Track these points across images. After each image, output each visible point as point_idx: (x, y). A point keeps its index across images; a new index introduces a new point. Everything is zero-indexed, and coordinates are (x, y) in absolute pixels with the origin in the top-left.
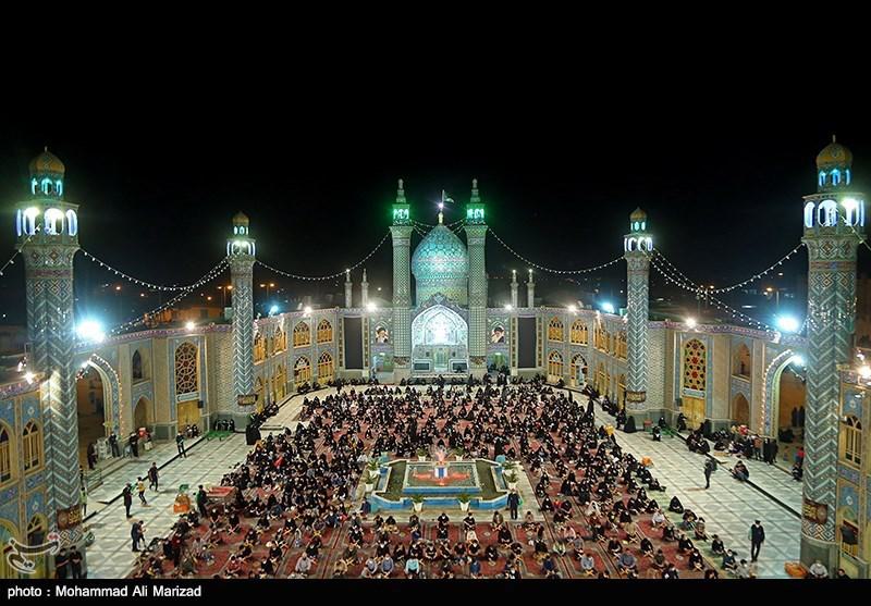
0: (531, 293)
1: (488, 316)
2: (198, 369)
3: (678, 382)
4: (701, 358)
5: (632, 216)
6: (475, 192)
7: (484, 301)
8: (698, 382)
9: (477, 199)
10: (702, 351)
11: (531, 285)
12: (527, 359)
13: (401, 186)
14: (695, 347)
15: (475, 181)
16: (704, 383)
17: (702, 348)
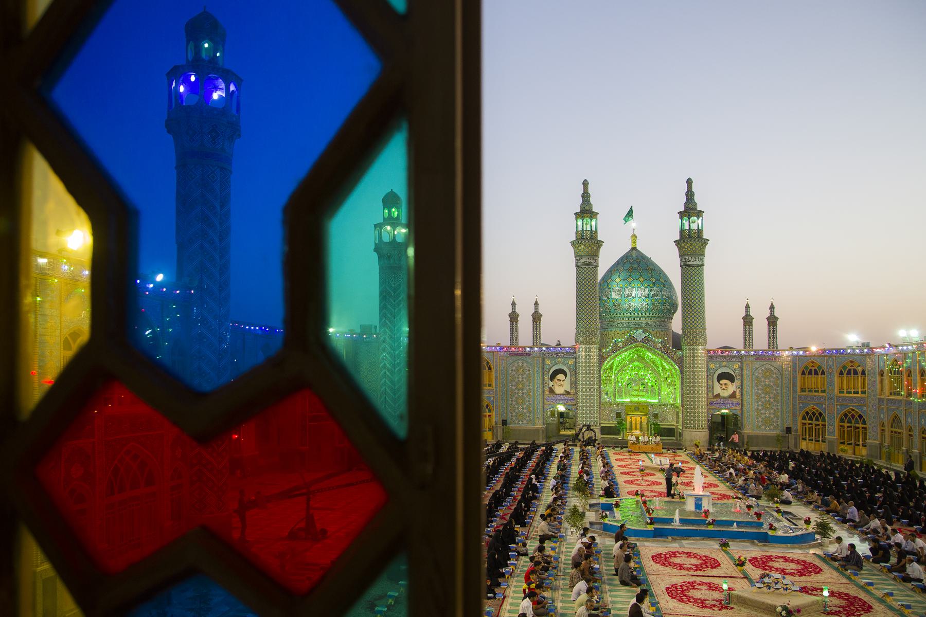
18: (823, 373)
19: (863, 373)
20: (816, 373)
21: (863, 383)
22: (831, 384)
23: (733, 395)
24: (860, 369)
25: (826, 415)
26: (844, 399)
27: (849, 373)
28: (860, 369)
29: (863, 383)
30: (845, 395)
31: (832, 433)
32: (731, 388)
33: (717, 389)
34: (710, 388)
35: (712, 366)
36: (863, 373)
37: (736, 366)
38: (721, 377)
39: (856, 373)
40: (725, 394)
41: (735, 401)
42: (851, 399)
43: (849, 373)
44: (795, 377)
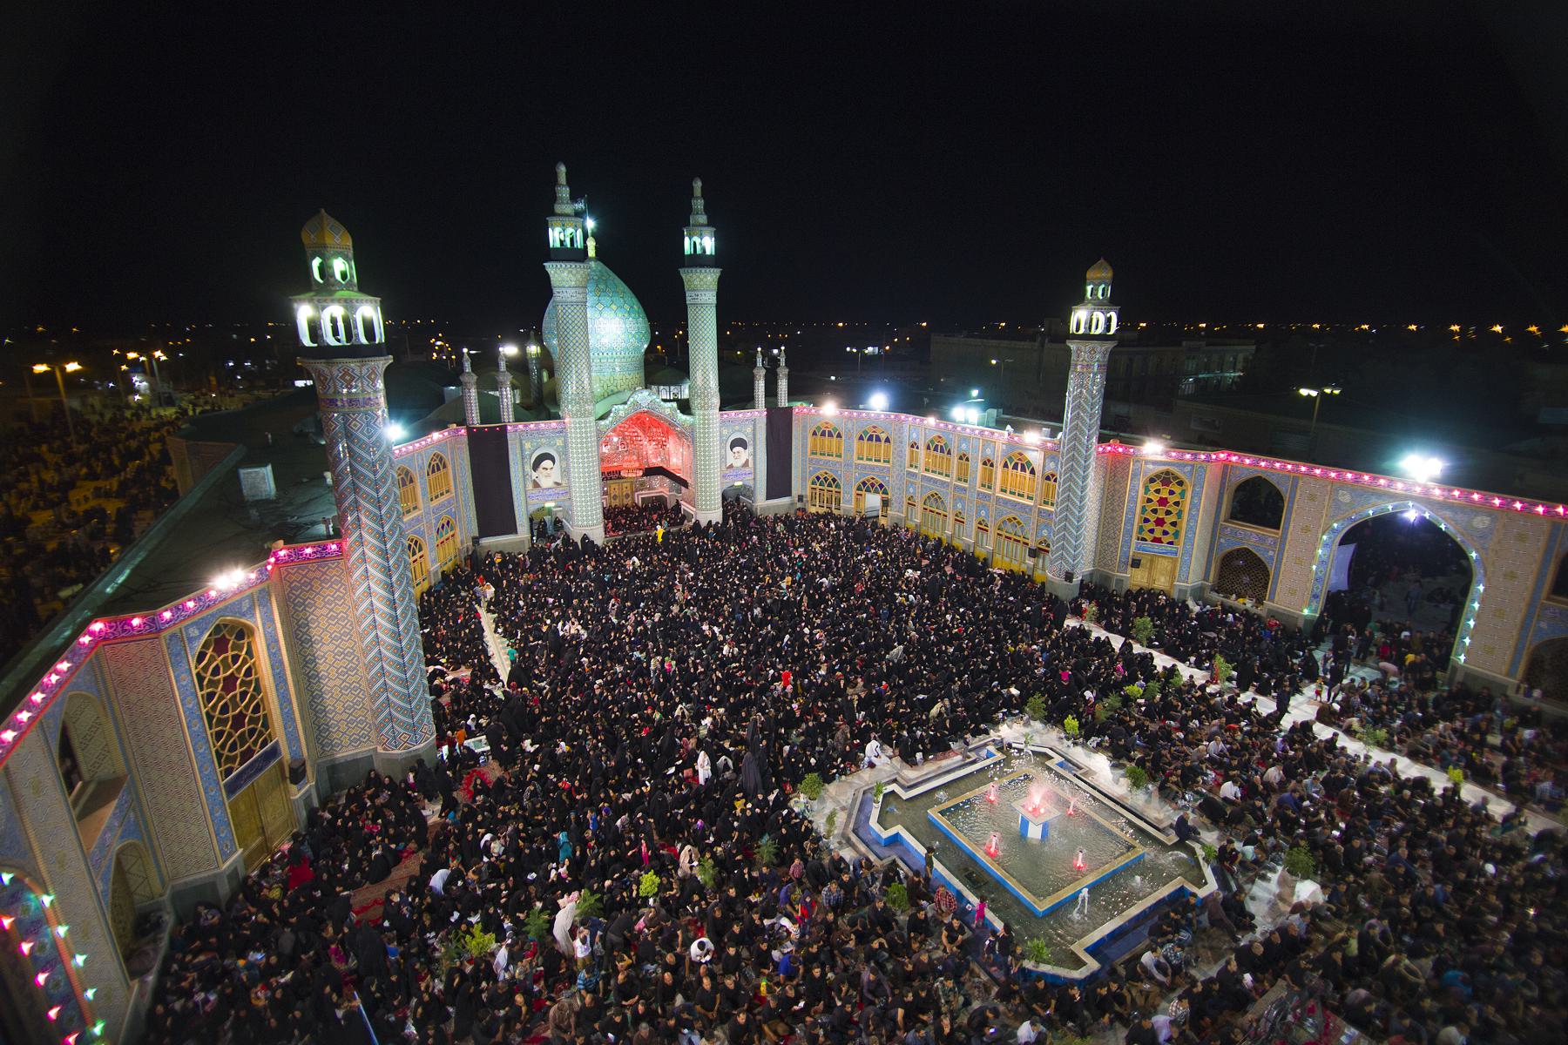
0: (783, 385)
1: (723, 422)
2: (268, 682)
3: (1129, 533)
4: (1172, 499)
5: (1090, 275)
6: (699, 204)
7: (716, 401)
8: (1166, 533)
9: (703, 219)
10: (1177, 489)
11: (783, 372)
12: (779, 483)
13: (562, 178)
14: (1166, 482)
15: (698, 185)
16: (1177, 534)
17: (1181, 483)
18: (839, 436)
19: (887, 440)
20: (830, 435)
21: (887, 452)
22: (849, 450)
23: (746, 464)
24: (883, 436)
25: (842, 482)
26: (864, 467)
27: (870, 438)
28: (883, 436)
29: (887, 452)
30: (865, 462)
31: (849, 501)
32: (743, 455)
33: (731, 460)
34: (723, 458)
35: (725, 432)
36: (887, 440)
37: (749, 430)
38: (739, 443)
39: (878, 439)
40: (738, 463)
41: (747, 470)
42: (872, 468)
43: (870, 438)
44: (804, 438)
